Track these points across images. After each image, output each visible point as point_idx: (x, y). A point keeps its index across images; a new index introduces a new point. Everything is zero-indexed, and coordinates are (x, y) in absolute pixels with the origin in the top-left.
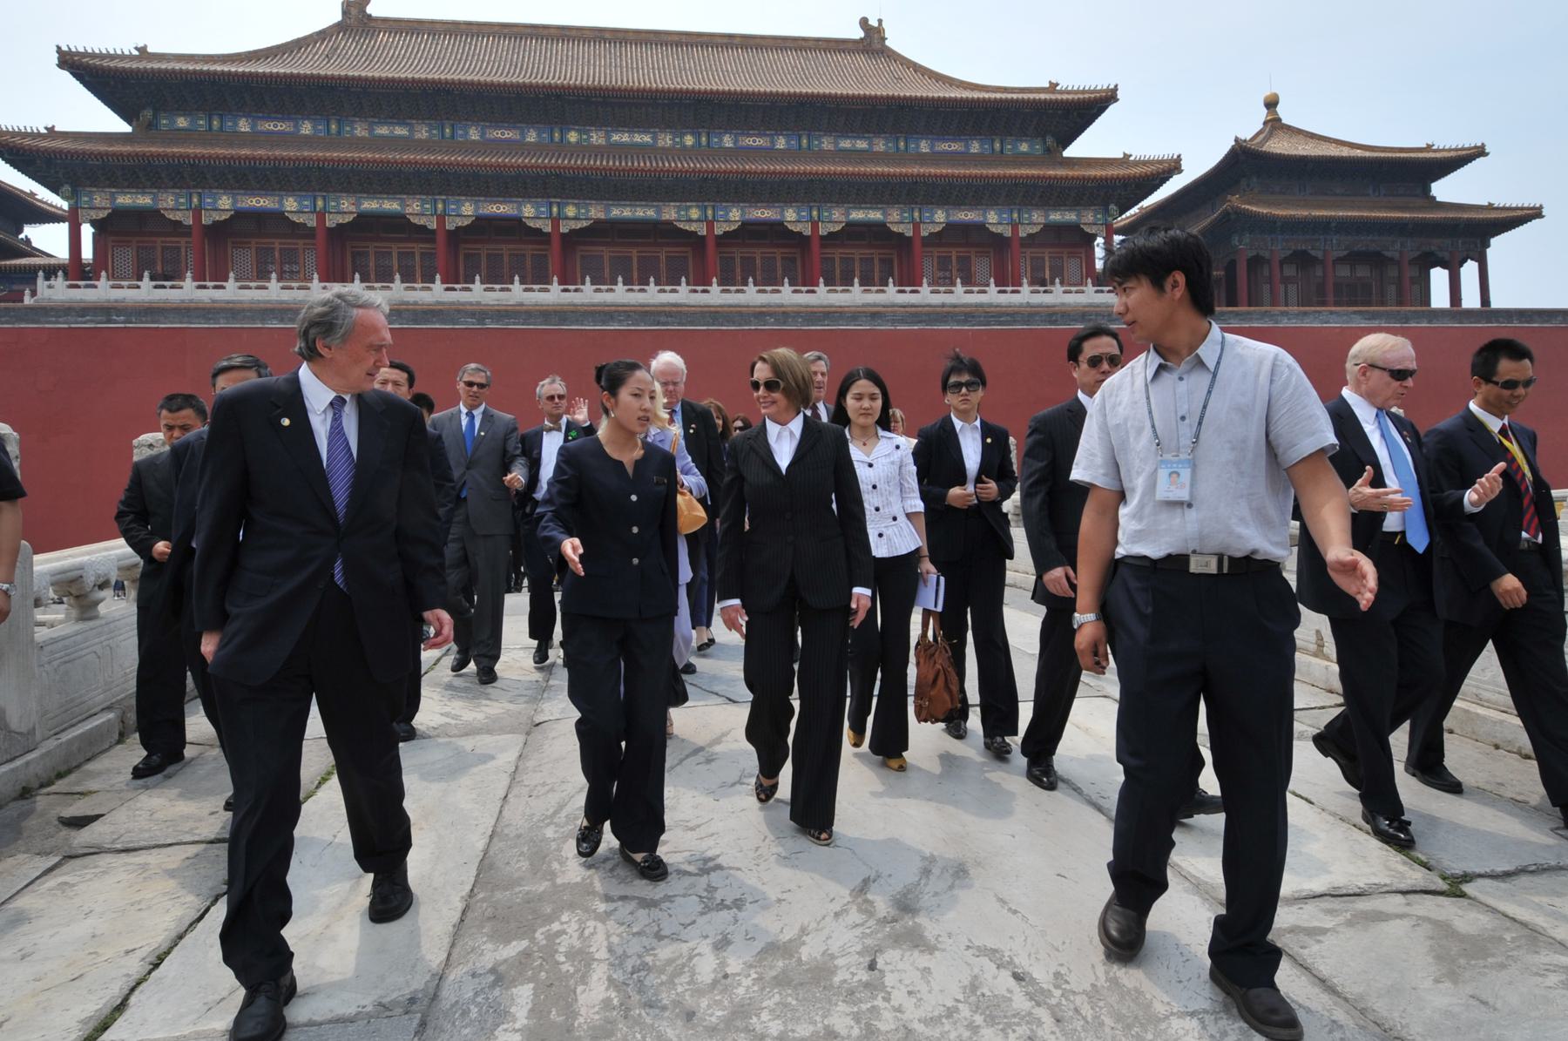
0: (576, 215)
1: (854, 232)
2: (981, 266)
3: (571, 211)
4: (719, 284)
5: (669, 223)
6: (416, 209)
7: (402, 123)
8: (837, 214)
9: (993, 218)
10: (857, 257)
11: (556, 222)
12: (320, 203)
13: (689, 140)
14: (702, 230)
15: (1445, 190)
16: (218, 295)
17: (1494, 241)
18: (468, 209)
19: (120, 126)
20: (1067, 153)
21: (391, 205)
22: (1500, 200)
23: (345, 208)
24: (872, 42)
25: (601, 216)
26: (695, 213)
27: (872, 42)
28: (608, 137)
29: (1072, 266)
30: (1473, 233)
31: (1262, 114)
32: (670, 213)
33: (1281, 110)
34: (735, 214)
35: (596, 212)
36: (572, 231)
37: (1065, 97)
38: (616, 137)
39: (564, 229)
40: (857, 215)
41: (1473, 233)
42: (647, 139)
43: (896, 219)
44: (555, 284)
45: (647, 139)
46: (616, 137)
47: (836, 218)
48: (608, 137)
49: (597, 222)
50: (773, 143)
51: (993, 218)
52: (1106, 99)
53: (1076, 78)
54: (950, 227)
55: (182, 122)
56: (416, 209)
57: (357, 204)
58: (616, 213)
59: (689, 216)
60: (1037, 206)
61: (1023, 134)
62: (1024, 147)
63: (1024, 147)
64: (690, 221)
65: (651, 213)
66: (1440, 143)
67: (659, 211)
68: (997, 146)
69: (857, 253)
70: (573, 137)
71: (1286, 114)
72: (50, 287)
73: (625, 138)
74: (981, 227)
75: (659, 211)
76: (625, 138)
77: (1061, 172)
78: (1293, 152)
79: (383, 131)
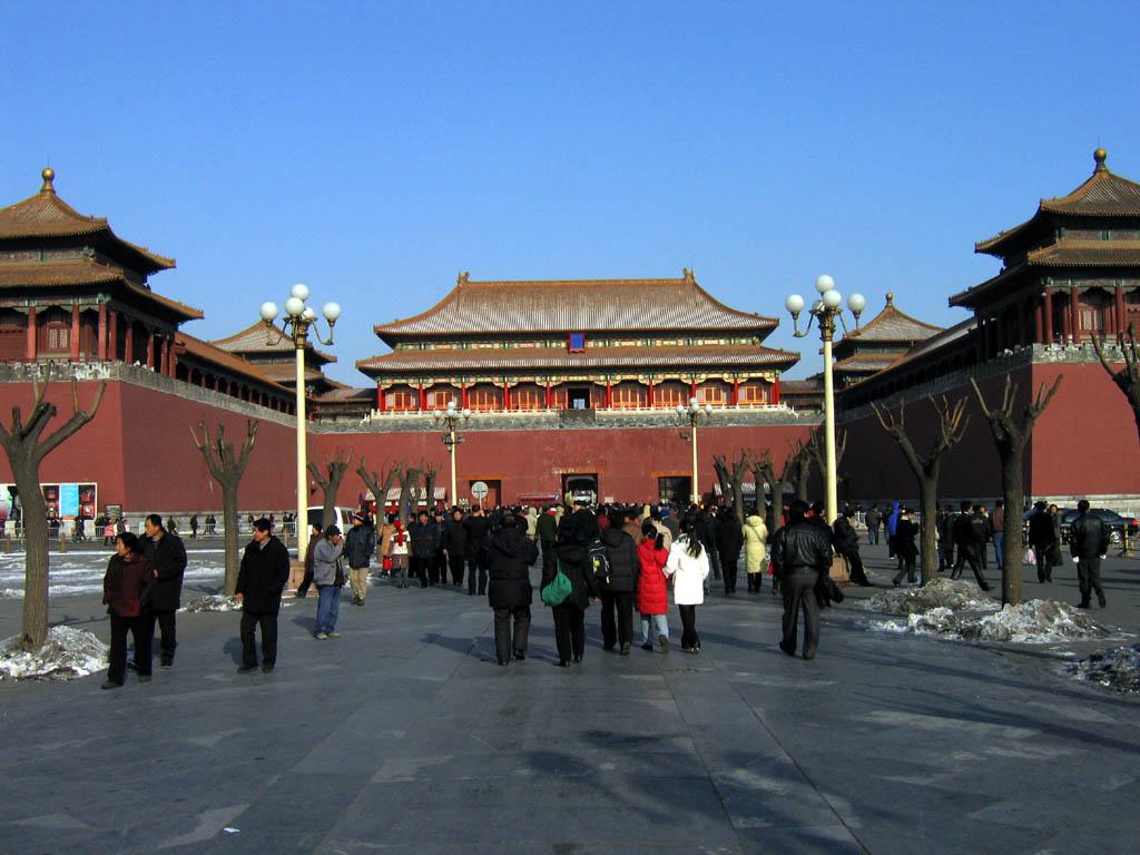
3: (554, 378)
5: (591, 383)
6: (497, 381)
9: (726, 376)
11: (548, 384)
13: (601, 344)
26: (602, 378)
32: (591, 378)
35: (564, 379)
39: (551, 385)
40: (668, 376)
51: (726, 376)
55: (410, 347)
56: (497, 381)
58: (571, 378)
62: (744, 341)
65: (585, 378)
70: (554, 345)
79: (482, 346)
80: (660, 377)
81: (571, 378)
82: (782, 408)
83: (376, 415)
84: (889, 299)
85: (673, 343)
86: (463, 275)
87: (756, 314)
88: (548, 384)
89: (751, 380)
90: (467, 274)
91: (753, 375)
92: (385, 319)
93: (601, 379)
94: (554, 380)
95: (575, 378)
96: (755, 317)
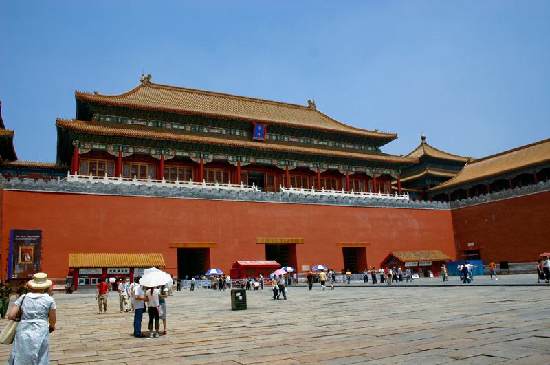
0: (245, 161)
3: (244, 159)
4: (179, 180)
8: (325, 166)
13: (274, 138)
18: (211, 157)
25: (254, 162)
26: (283, 163)
31: (420, 141)
32: (275, 162)
33: (426, 141)
35: (252, 160)
36: (244, 166)
37: (380, 135)
44: (76, 174)
52: (395, 137)
53: (384, 129)
54: (356, 173)
58: (258, 161)
61: (370, 145)
62: (370, 149)
63: (370, 149)
64: (281, 165)
65: (269, 162)
67: (271, 161)
68: (363, 148)
69: (215, 171)
72: (72, 177)
74: (364, 174)
77: (379, 157)
78: (437, 156)
80: (325, 167)
81: (258, 161)
84: (423, 138)
86: (146, 76)
87: (377, 131)
90: (149, 77)
91: (384, 172)
92: (89, 90)
93: (281, 164)
94: (245, 161)
95: (262, 161)
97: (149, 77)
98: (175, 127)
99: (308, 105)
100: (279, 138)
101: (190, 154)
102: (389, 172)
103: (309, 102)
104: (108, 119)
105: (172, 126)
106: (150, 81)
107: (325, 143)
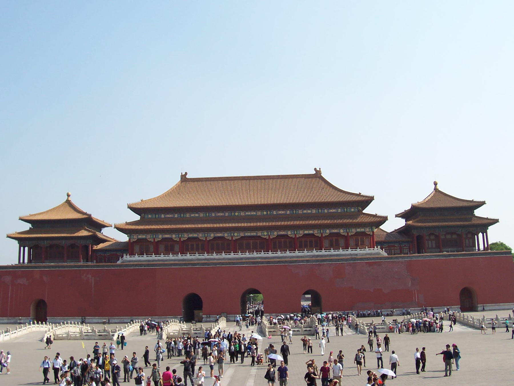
0: (237, 235)
1: (305, 235)
2: (342, 242)
3: (236, 234)
5: (259, 236)
6: (200, 236)
7: (197, 213)
10: (308, 240)
11: (232, 237)
12: (180, 235)
13: (265, 213)
14: (268, 238)
15: (478, 212)
16: (159, 258)
17: (489, 228)
19: (137, 218)
20: (364, 211)
21: (195, 235)
22: (490, 217)
23: (186, 236)
24: (318, 175)
26: (266, 233)
27: (318, 175)
28: (245, 213)
29: (367, 241)
30: (485, 225)
32: (259, 234)
33: (439, 187)
34: (276, 233)
35: (242, 234)
38: (247, 213)
41: (485, 225)
42: (255, 213)
43: (316, 232)
45: (255, 213)
46: (247, 213)
47: (301, 233)
48: (245, 213)
49: (242, 237)
50: (286, 212)
53: (366, 192)
54: (330, 234)
55: (150, 216)
56: (200, 236)
57: (188, 235)
58: (246, 234)
59: (265, 234)
60: (354, 228)
62: (353, 210)
63: (353, 210)
66: (476, 200)
67: (257, 234)
70: (237, 214)
71: (440, 188)
73: (249, 213)
75: (257, 234)
76: (249, 213)
79: (193, 215)
80: (301, 233)
82: (377, 250)
83: (127, 258)
84: (435, 184)
85: (309, 211)
88: (232, 237)
89: (357, 234)
90: (186, 173)
91: (358, 230)
92: (135, 200)
95: (249, 234)
96: (359, 195)
97: (186, 173)
98: (193, 215)
99: (315, 172)
100: (269, 212)
101: (198, 235)
102: (363, 230)
103: (315, 169)
104: (150, 216)
105: (190, 215)
106: (188, 177)
107: (309, 211)
